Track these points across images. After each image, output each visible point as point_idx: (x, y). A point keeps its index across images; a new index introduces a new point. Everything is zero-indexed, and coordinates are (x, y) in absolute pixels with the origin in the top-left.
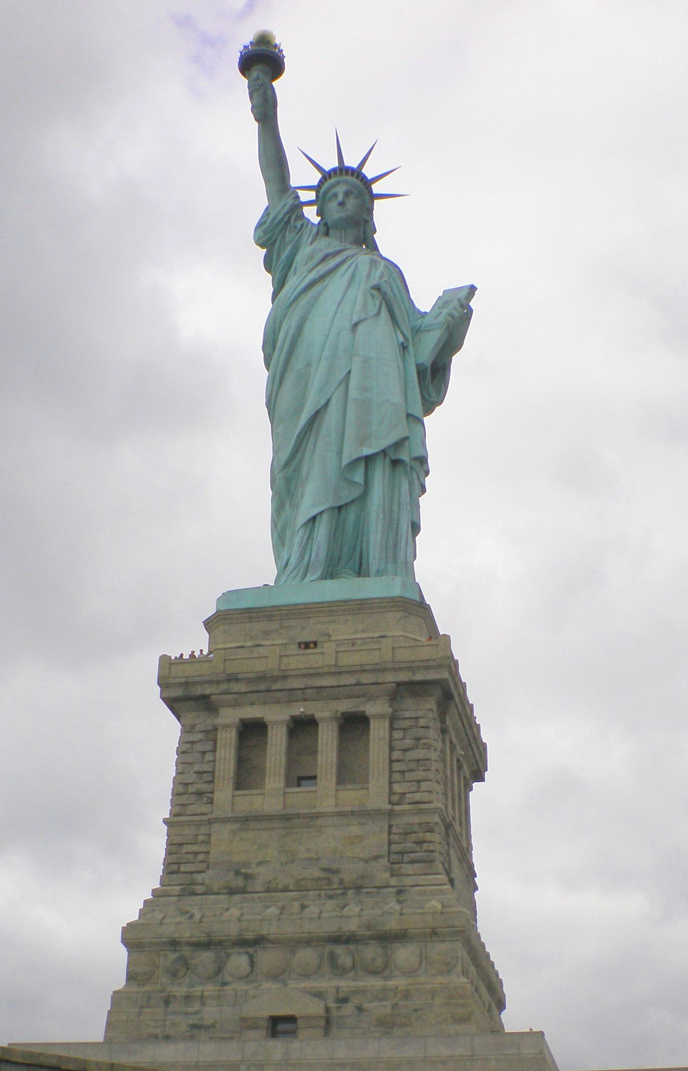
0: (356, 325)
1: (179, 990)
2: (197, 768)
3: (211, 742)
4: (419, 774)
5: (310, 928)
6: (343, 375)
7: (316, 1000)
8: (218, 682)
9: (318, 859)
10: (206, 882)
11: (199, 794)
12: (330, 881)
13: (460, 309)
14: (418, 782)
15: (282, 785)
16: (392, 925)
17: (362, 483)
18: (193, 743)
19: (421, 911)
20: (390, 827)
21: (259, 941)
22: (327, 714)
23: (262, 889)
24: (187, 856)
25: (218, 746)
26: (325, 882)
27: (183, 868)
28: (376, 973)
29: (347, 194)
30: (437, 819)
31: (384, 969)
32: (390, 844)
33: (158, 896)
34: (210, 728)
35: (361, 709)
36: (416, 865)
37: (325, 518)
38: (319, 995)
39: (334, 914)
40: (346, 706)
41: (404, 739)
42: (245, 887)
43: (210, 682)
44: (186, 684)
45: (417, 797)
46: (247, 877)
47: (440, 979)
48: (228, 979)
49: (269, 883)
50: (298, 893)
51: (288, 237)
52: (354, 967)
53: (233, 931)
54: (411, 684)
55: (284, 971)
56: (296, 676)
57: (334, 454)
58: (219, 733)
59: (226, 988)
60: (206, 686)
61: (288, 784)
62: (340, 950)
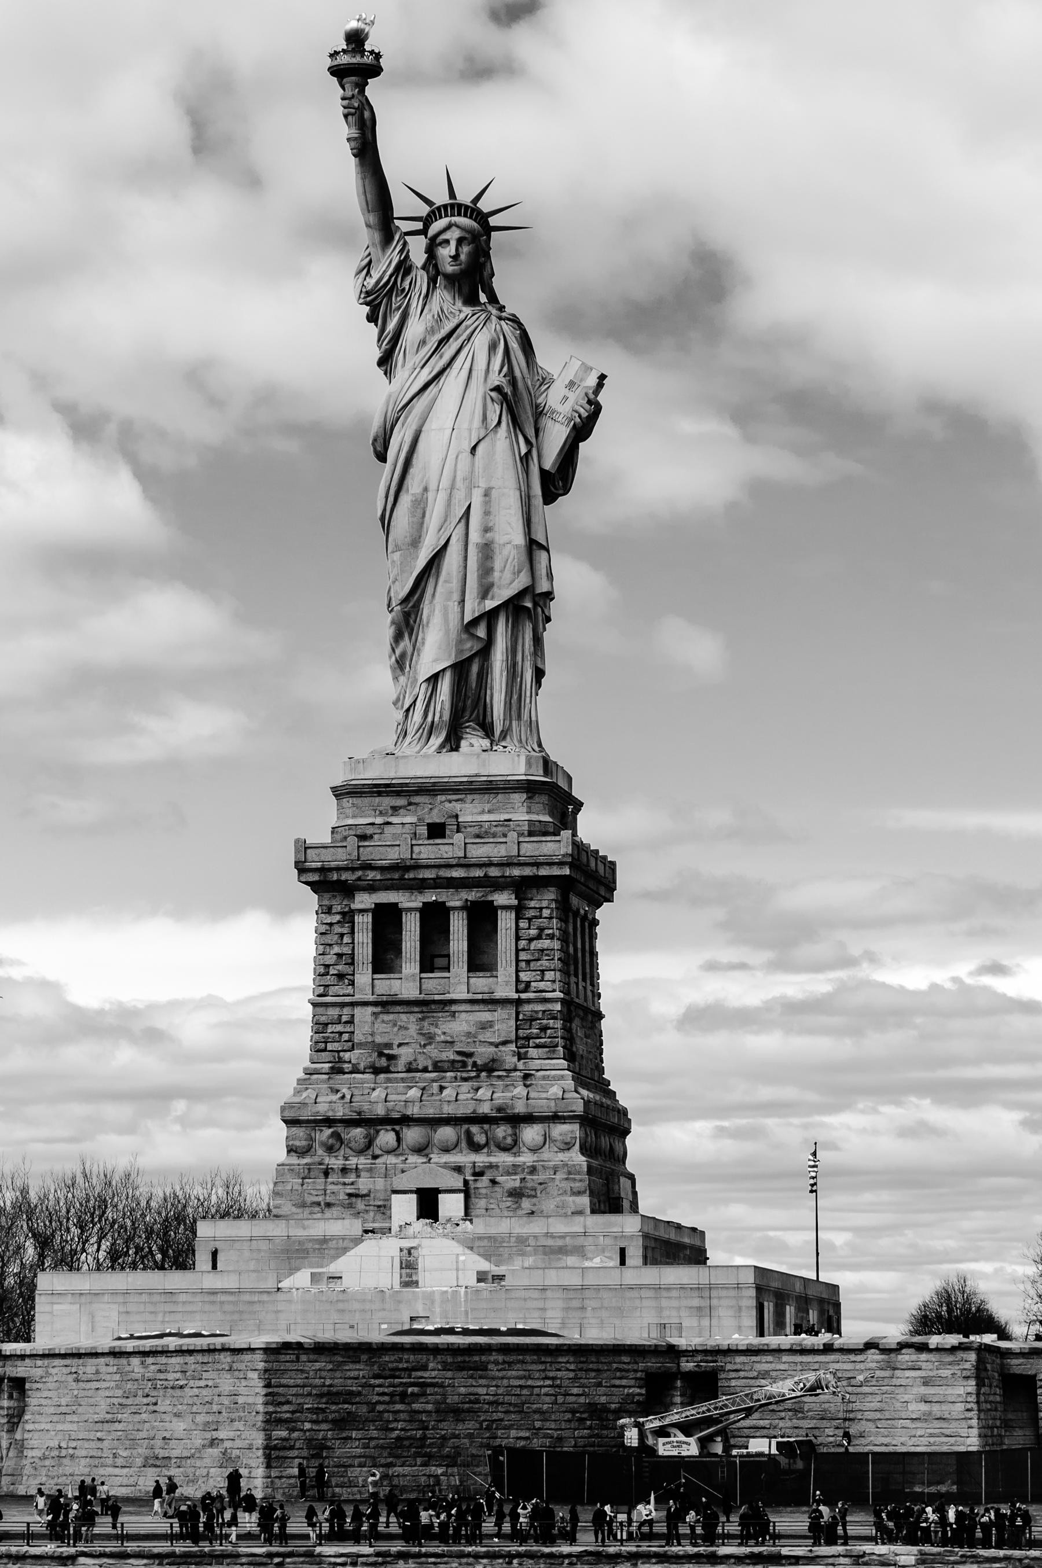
0: (474, 449)
1: (335, 1162)
2: (336, 949)
3: (347, 925)
4: (544, 963)
5: (448, 1110)
6: (465, 508)
7: (456, 1175)
8: (353, 869)
9: (452, 1043)
10: (353, 1061)
11: (341, 976)
12: (464, 1064)
13: (587, 407)
14: (543, 971)
15: (418, 970)
16: (520, 1108)
17: (486, 638)
18: (331, 924)
19: (544, 1095)
20: (517, 1014)
21: (406, 1120)
22: (458, 904)
23: (404, 1070)
24: (334, 1035)
25: (356, 930)
26: (460, 1064)
27: (330, 1047)
28: (505, 1149)
29: (460, 241)
30: (558, 1007)
31: (513, 1147)
32: (517, 1029)
33: (310, 1074)
34: (347, 909)
35: (490, 898)
36: (540, 1050)
37: (448, 675)
38: (458, 1169)
39: (470, 1096)
40: (473, 895)
41: (529, 928)
42: (389, 1066)
43: (346, 869)
44: (322, 870)
45: (542, 985)
46: (391, 1058)
47: (561, 1156)
48: (378, 1152)
49: (410, 1063)
50: (437, 1074)
51: (396, 301)
52: (487, 1144)
53: (380, 1111)
54: (536, 878)
55: (428, 1146)
56: (428, 867)
57: (456, 603)
58: (356, 917)
59: (377, 1161)
60: (342, 872)
61: (421, 971)
62: (475, 1129)
